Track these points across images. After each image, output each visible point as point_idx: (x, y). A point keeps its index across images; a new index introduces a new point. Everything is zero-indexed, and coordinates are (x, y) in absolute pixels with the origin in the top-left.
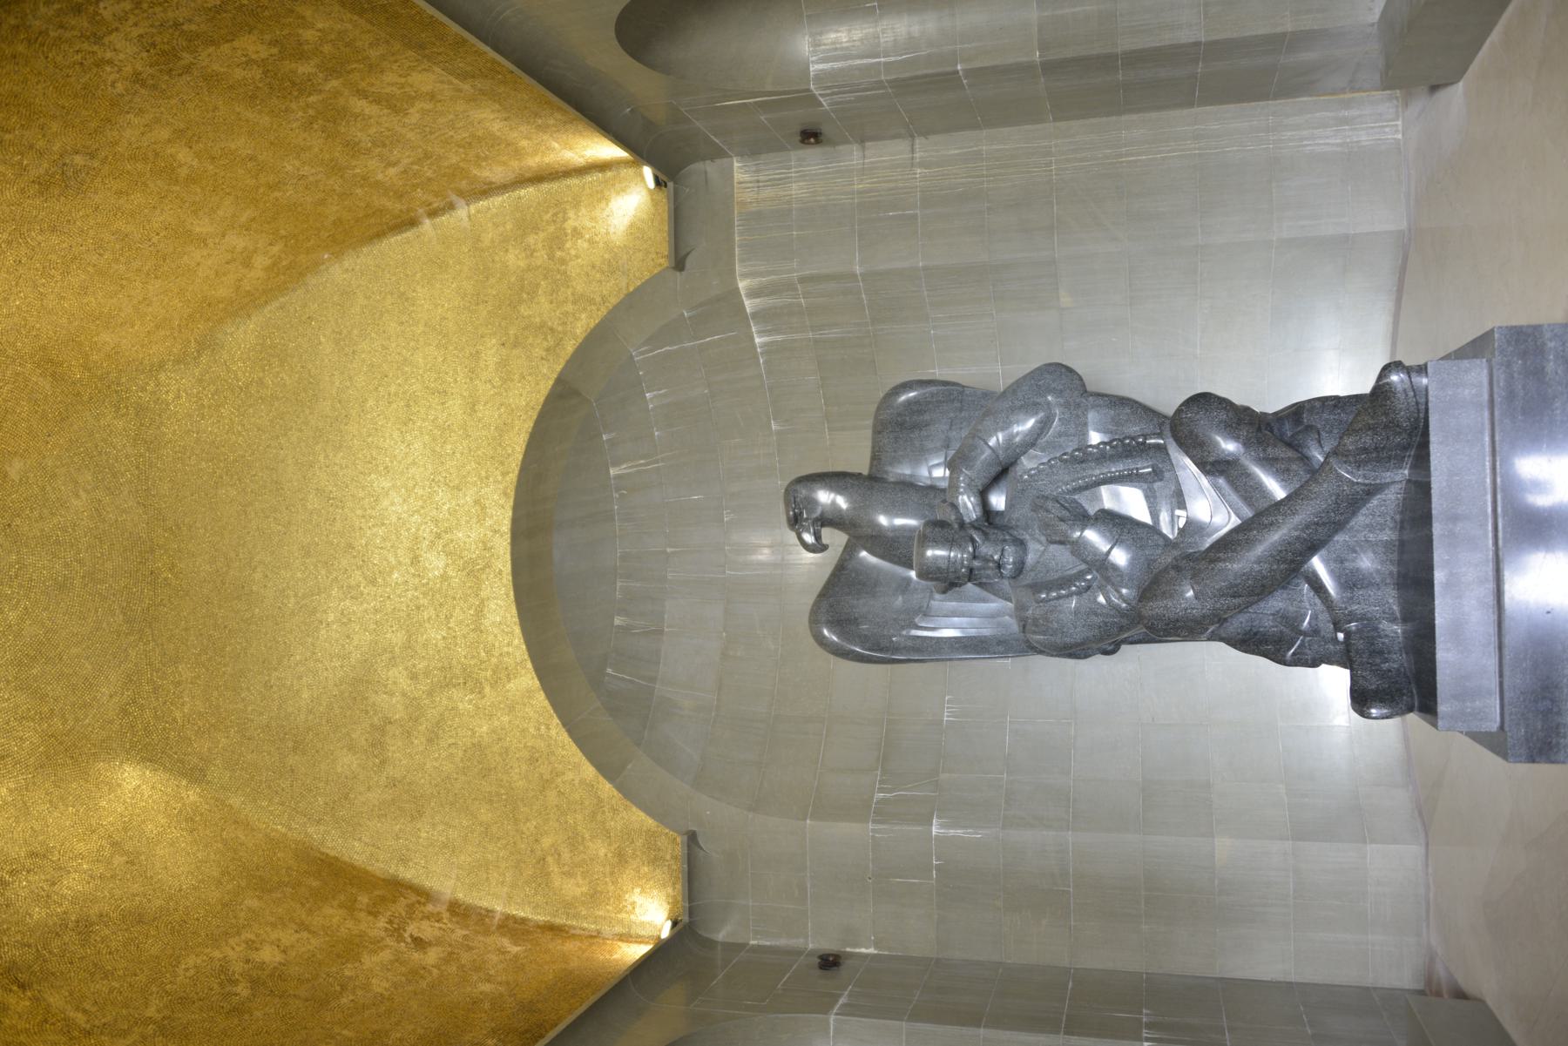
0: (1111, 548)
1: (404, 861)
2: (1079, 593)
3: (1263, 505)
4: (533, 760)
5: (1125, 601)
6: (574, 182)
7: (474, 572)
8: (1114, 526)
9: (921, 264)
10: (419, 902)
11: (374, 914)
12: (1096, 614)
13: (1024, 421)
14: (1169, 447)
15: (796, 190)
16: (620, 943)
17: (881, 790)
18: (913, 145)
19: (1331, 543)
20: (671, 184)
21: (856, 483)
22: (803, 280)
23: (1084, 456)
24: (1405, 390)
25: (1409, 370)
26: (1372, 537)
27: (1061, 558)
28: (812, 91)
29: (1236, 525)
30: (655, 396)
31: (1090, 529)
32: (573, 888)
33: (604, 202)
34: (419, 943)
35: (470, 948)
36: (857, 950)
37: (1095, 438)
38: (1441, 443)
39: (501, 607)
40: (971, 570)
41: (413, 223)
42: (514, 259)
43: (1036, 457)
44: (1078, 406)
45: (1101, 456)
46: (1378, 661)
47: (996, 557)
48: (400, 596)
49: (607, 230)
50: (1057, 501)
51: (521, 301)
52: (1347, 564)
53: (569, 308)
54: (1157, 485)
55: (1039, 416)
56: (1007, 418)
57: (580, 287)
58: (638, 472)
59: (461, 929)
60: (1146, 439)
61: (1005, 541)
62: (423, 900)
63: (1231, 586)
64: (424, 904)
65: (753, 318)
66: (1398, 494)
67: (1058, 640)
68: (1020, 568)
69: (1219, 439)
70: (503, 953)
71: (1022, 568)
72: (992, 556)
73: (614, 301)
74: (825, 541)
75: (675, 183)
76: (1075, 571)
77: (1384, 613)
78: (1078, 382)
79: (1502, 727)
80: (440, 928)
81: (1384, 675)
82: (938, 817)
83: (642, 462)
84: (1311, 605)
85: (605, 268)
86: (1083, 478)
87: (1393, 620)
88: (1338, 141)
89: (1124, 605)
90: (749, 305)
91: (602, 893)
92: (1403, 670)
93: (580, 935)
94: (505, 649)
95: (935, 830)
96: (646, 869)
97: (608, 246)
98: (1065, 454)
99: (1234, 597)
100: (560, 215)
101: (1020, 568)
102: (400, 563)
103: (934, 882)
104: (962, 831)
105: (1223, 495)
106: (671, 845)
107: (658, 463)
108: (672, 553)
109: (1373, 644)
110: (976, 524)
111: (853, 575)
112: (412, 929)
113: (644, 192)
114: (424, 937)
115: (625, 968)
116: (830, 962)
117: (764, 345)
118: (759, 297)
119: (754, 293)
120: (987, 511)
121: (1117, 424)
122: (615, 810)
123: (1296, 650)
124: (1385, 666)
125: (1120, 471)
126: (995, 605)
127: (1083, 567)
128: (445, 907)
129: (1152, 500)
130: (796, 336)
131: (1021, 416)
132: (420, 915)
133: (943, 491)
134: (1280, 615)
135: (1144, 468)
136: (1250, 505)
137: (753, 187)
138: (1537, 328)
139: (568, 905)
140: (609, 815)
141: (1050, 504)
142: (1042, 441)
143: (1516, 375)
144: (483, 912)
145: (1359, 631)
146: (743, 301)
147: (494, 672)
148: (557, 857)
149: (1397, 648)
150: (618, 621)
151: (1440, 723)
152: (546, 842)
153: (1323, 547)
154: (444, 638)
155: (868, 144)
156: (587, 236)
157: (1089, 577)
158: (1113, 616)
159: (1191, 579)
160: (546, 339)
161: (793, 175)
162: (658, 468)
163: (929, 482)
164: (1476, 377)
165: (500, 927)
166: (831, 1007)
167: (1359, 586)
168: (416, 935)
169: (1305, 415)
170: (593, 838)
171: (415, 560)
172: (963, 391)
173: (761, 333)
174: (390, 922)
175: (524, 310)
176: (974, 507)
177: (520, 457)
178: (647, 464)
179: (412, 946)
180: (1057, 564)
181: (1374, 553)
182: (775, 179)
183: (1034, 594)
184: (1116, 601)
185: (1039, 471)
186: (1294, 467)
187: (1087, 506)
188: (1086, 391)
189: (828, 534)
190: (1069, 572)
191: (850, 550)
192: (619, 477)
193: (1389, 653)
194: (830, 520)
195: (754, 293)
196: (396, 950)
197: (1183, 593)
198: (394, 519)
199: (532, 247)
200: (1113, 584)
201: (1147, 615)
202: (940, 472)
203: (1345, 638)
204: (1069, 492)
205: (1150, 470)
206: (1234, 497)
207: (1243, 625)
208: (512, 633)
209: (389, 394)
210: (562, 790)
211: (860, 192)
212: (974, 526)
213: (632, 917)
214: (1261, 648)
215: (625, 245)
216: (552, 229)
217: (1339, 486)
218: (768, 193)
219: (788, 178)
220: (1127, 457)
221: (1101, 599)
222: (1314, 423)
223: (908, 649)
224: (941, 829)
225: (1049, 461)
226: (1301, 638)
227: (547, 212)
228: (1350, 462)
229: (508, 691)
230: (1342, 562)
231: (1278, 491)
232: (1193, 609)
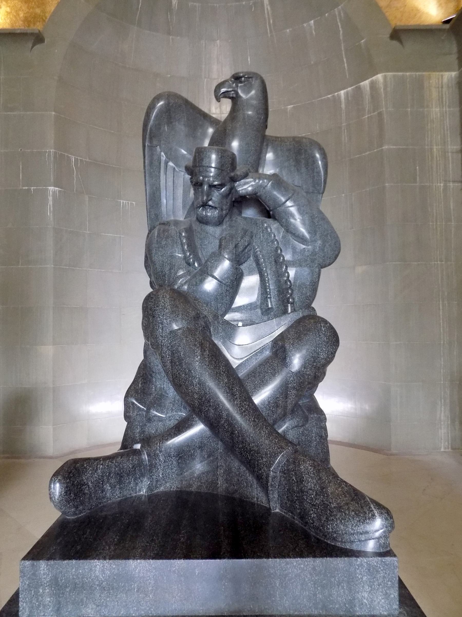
0: (216, 278)
2: (185, 258)
3: (249, 386)
5: (179, 288)
8: (232, 281)
12: (170, 269)
13: (304, 223)
17: (76, 160)
18: (457, 181)
20: (447, 26)
21: (261, 121)
22: (380, 114)
24: (367, 532)
30: (311, 27)
31: (230, 264)
37: (292, 272)
38: (314, 569)
44: (313, 261)
46: (113, 481)
47: (210, 203)
54: (259, 311)
56: (307, 213)
61: (222, 210)
63: (180, 360)
65: (356, 87)
66: (257, 499)
67: (154, 245)
68: (203, 221)
71: (203, 223)
72: (211, 200)
76: (200, 256)
77: (157, 481)
78: (328, 262)
81: (100, 484)
82: (59, 191)
83: (271, 22)
87: (150, 488)
88: (442, 418)
90: (366, 83)
95: (51, 188)
98: (281, 250)
99: (171, 362)
101: (203, 221)
103: (21, 188)
105: (256, 354)
107: (270, 33)
109: (128, 475)
111: (200, 123)
117: (339, 97)
118: (370, 88)
119: (373, 86)
121: (300, 286)
123: (136, 405)
125: (269, 286)
127: (203, 261)
129: (249, 307)
130: (344, 115)
131: (307, 222)
133: (257, 171)
134: (163, 394)
135: (271, 302)
136: (248, 375)
141: (247, 238)
142: (290, 237)
145: (141, 462)
146: (368, 79)
149: (125, 493)
151: (28, 563)
153: (213, 434)
157: (196, 265)
158: (169, 280)
159: (188, 328)
161: (444, 109)
162: (267, 33)
167: (180, 461)
169: (315, 415)
172: (320, 193)
173: (347, 94)
176: (245, 189)
180: (205, 245)
181: (208, 472)
184: (180, 281)
185: (269, 233)
186: (279, 411)
188: (322, 268)
200: (190, 279)
201: (159, 293)
203: (136, 449)
204: (255, 253)
205: (270, 306)
206: (254, 363)
207: (156, 367)
211: (431, 149)
212: (232, 190)
214: (140, 379)
215: (406, 6)
217: (266, 454)
218: (435, 94)
220: (279, 291)
221: (181, 273)
222: (309, 422)
223: (152, 156)
225: (276, 240)
226: (145, 409)
228: (288, 466)
230: (200, 447)
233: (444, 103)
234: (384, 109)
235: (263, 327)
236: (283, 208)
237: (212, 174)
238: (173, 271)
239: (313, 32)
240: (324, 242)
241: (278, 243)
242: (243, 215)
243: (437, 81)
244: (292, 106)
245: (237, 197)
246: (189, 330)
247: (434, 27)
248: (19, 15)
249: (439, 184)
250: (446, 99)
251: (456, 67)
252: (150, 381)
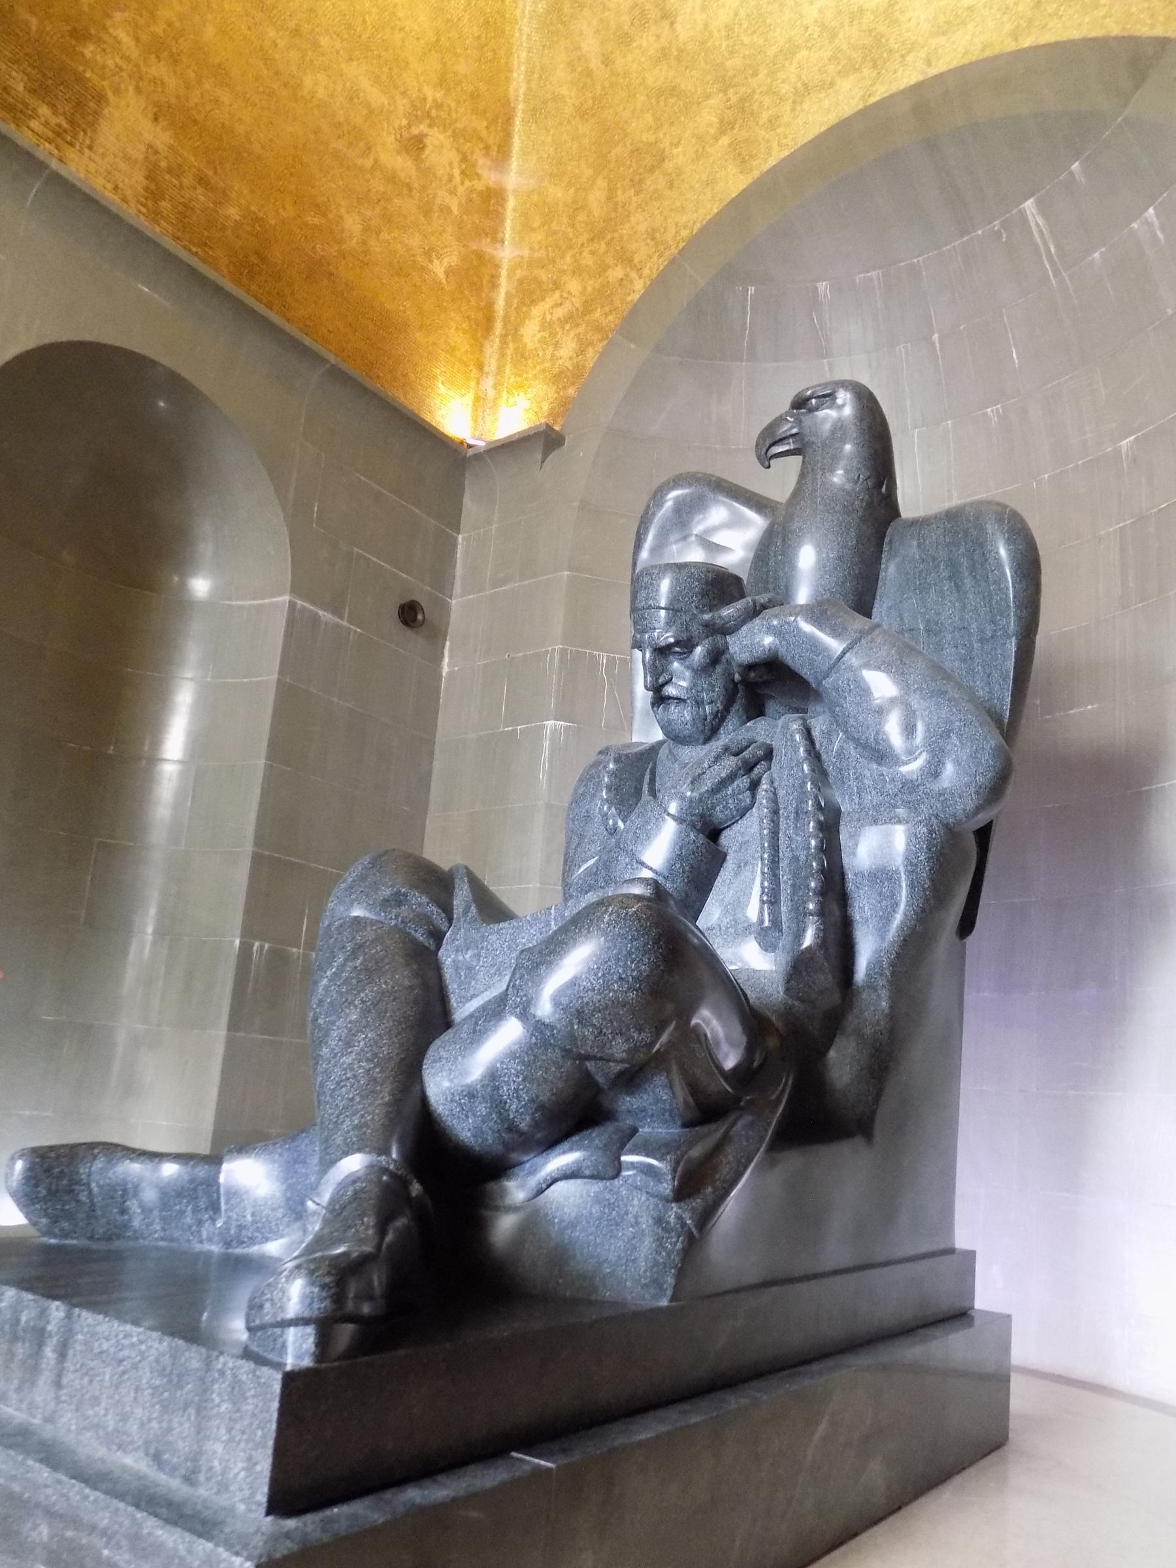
35: (427, 213)
59: (460, 205)
80: (451, 178)
83: (1053, 250)
107: (1055, 277)
108: (933, 345)
114: (427, 152)
150: (822, 286)
165: (480, 255)
239: (1159, 233)
244: (1132, 438)
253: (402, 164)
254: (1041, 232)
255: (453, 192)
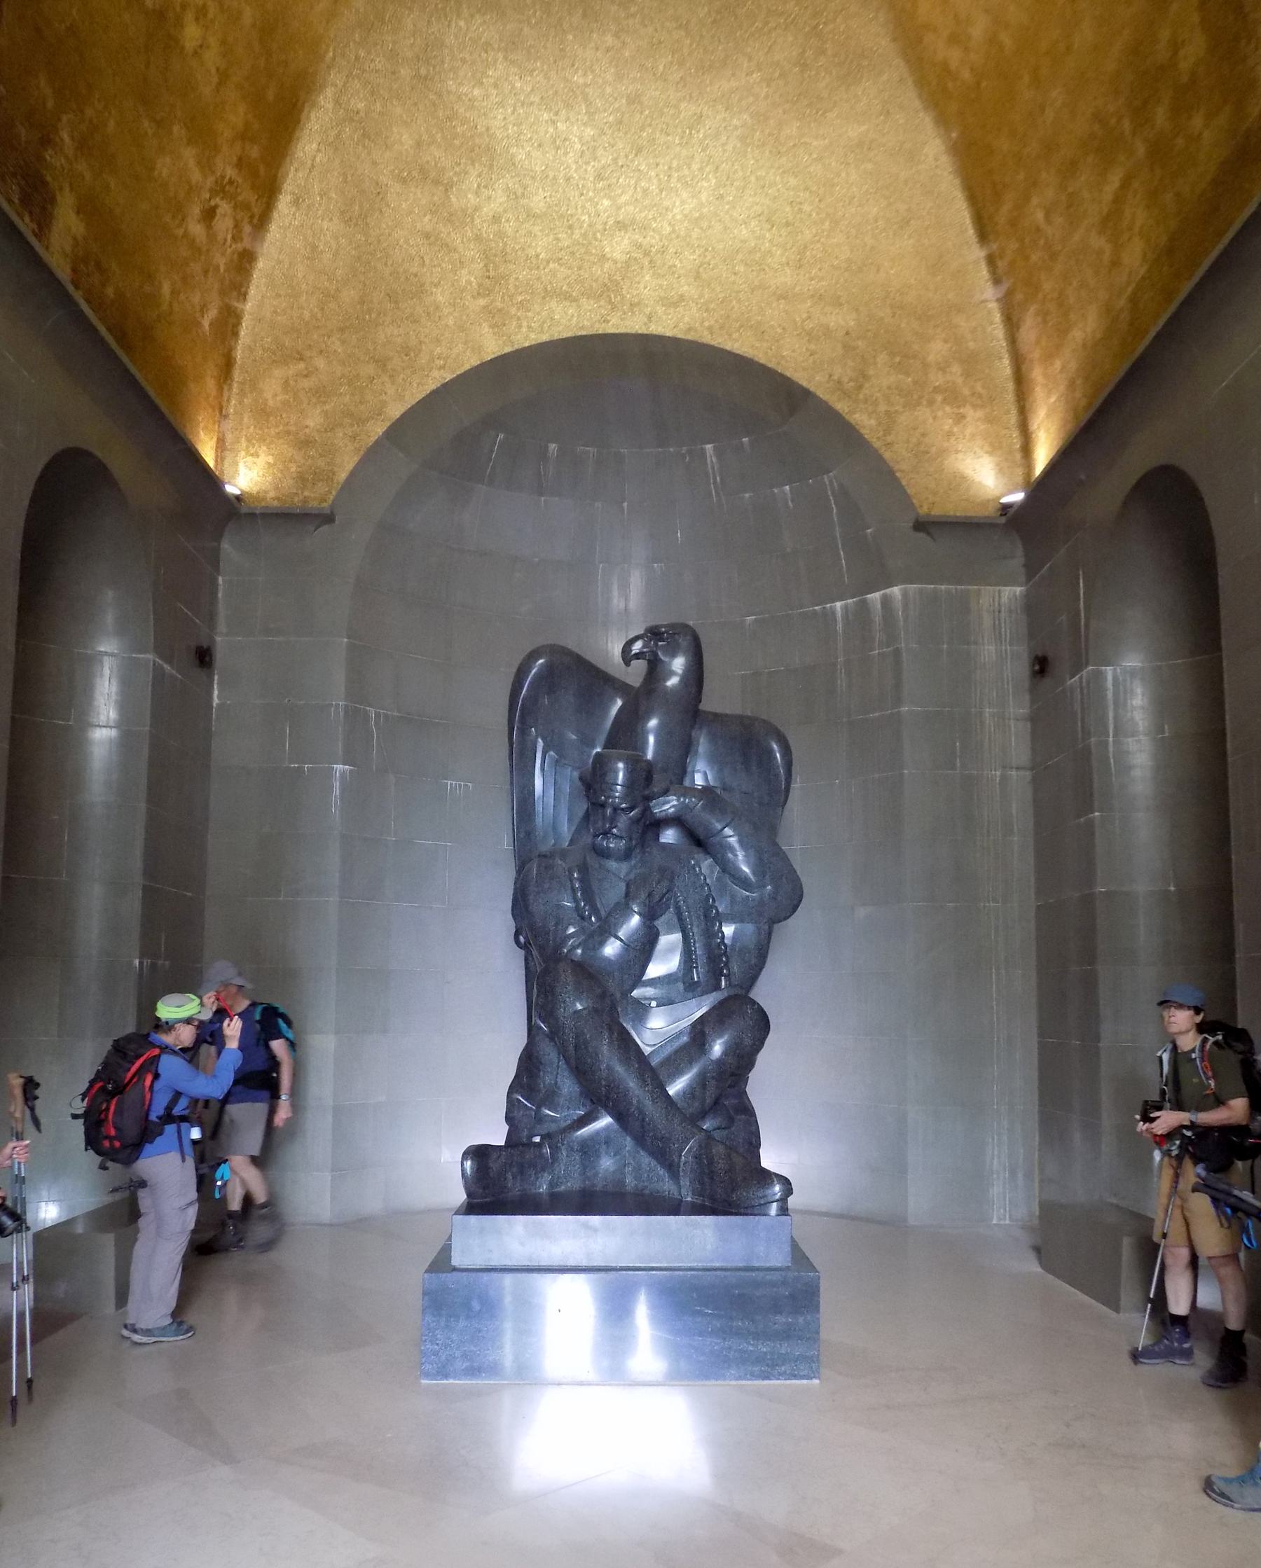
0: (621, 940)
1: (296, 202)
2: (577, 908)
4: (406, 350)
5: (569, 951)
6: (1013, 418)
7: (608, 291)
9: (906, 771)
10: (252, 217)
11: (240, 163)
12: (556, 924)
14: (720, 992)
15: (988, 651)
16: (215, 439)
19: (624, 1134)
22: (897, 653)
23: (711, 920)
24: (765, 1196)
25: (783, 1200)
26: (629, 1169)
27: (613, 893)
28: (1086, 667)
29: (644, 1050)
32: (272, 391)
33: (990, 450)
34: (209, 214)
35: (206, 272)
36: (215, 687)
37: (728, 930)
39: (570, 320)
40: (603, 806)
41: (983, 235)
42: (937, 349)
43: (712, 872)
44: (760, 914)
45: (711, 934)
46: (515, 1170)
48: (583, 207)
49: (960, 451)
50: (668, 891)
51: (892, 354)
52: (604, 1147)
53: (882, 408)
54: (681, 986)
55: (752, 877)
57: (904, 419)
58: (707, 474)
59: (225, 264)
60: (725, 976)
61: (631, 839)
62: (255, 221)
64: (251, 222)
66: (669, 1192)
67: (532, 888)
68: (603, 854)
69: (726, 1037)
70: (202, 311)
73: (887, 455)
74: (634, 663)
75: (1005, 525)
76: (599, 906)
79: (455, 1269)
80: (226, 240)
82: (351, 771)
84: (565, 1116)
85: (922, 448)
86: (690, 917)
89: (565, 951)
90: (875, 597)
91: (267, 421)
92: (506, 1190)
93: (222, 395)
94: (525, 324)
96: (293, 469)
97: (943, 452)
100: (979, 402)
101: (603, 854)
102: (619, 208)
103: (286, 764)
104: (338, 793)
106: (319, 496)
110: (648, 812)
112: (224, 207)
113: (997, 492)
114: (216, 220)
115: (192, 440)
116: (204, 657)
117: (833, 612)
119: (886, 601)
120: (659, 824)
122: (354, 438)
124: (509, 1176)
125: (695, 952)
126: (566, 830)
127: (603, 913)
128: (248, 246)
129: (666, 980)
132: (239, 217)
135: (698, 974)
137: (994, 605)
138: (818, 1311)
139: (253, 384)
140: (349, 431)
141: (665, 883)
143: (775, 1289)
144: (243, 290)
145: (542, 1156)
147: (500, 310)
148: (305, 372)
150: (553, 447)
152: (320, 363)
153: (621, 1127)
154: (537, 256)
155: (1029, 725)
156: (955, 429)
157: (593, 919)
158: (554, 940)
160: (851, 380)
163: (689, 769)
164: (778, 1257)
166: (161, 657)
168: (218, 211)
170: (326, 413)
171: (622, 226)
173: (846, 608)
174: (231, 182)
175: (882, 358)
176: (665, 810)
177: (728, 347)
178: (715, 482)
179: (206, 207)
180: (606, 889)
182: (1000, 628)
183: (577, 866)
185: (697, 875)
186: (697, 1104)
187: (662, 919)
188: (774, 923)
189: (640, 666)
190: (598, 900)
191: (622, 688)
192: (703, 452)
193: (522, 1180)
194: (655, 669)
195: (886, 601)
196: (201, 188)
197: (581, 1001)
198: (666, 203)
199: (948, 370)
202: (699, 781)
205: (696, 979)
206: (669, 1050)
208: (542, 332)
209: (801, 203)
210: (375, 381)
212: (647, 810)
213: (243, 453)
215: (944, 469)
216: (966, 392)
217: (678, 1140)
218: (987, 621)
219: (1001, 643)
220: (709, 958)
221: (571, 930)
222: (736, 1124)
223: (522, 742)
224: (340, 774)
227: (983, 387)
229: (480, 325)
230: (606, 1143)
231: (674, 1089)
232: (565, 1010)
233: (1003, 636)
234: (903, 645)
235: (680, 1008)
236: (718, 839)
237: (617, 794)
238: (560, 927)
240: (776, 888)
241: (709, 889)
242: (663, 840)
243: (991, 600)
245: (653, 821)
246: (596, 1011)
247: (982, 521)
248: (288, 469)
249: (993, 772)
250: (1006, 632)
251: (1023, 579)
252: (538, 1076)
253: (196, 229)
254: (713, 468)
255: (223, 254)
